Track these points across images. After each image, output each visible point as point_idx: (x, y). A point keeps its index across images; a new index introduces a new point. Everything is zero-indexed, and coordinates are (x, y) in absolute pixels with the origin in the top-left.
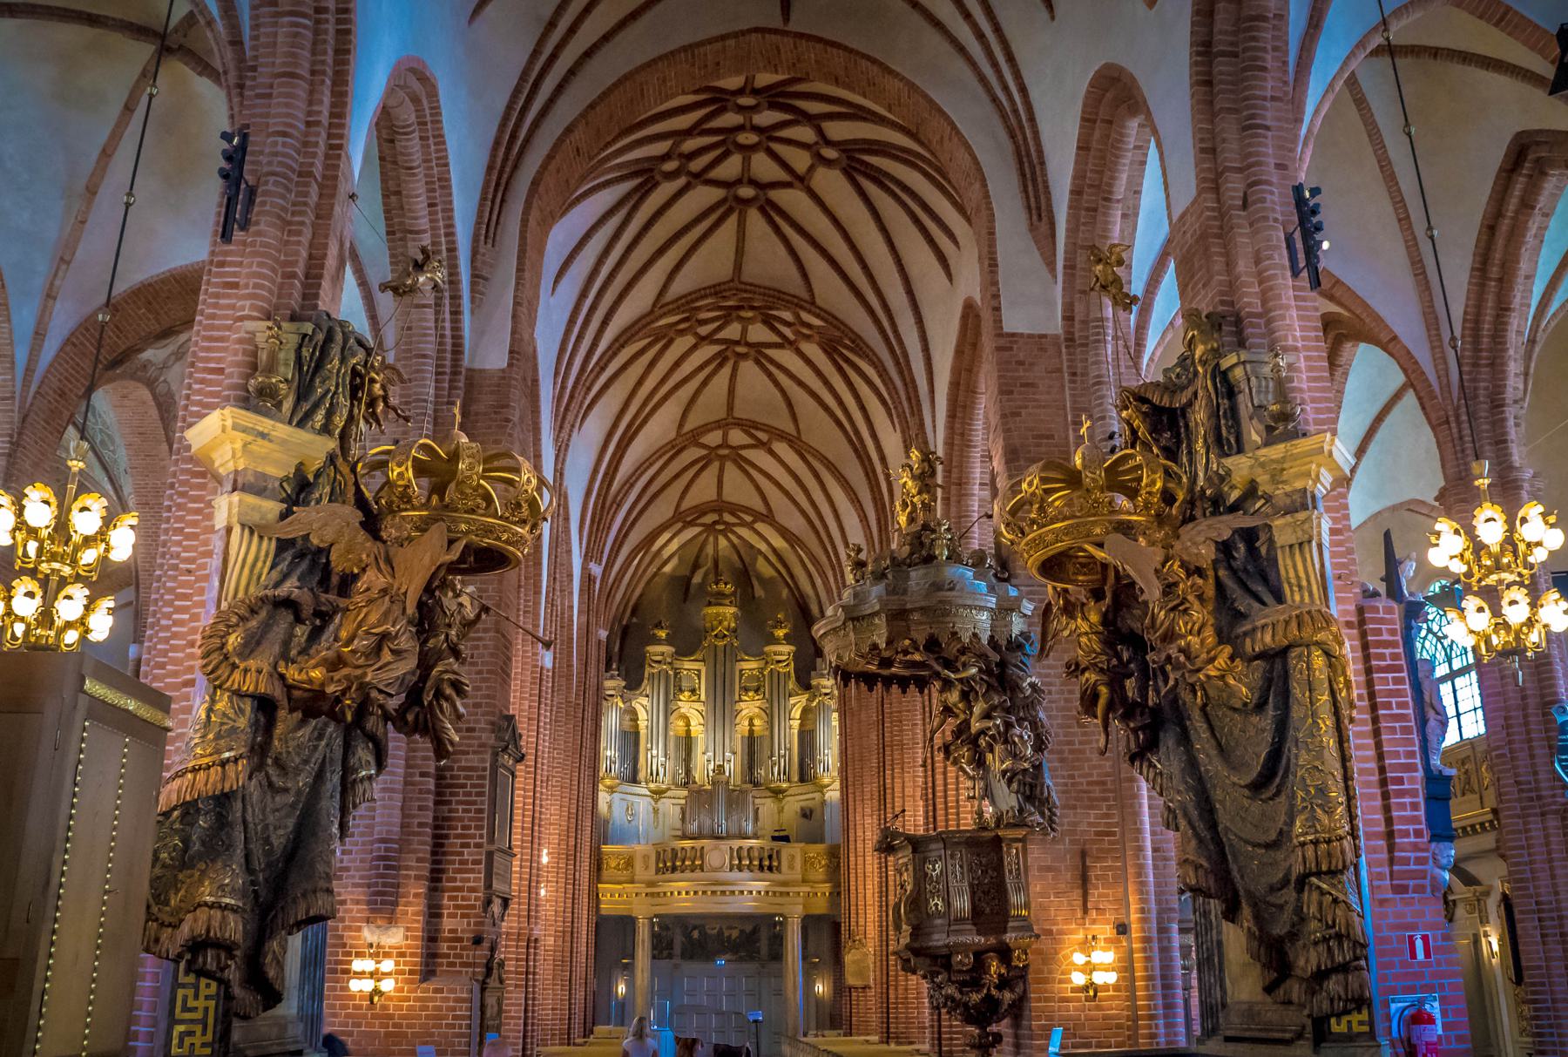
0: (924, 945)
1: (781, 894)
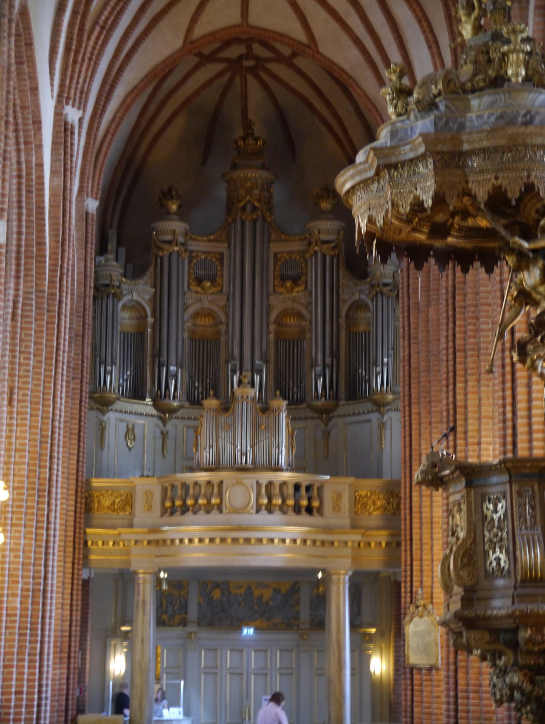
0: (480, 612)
1: (323, 543)
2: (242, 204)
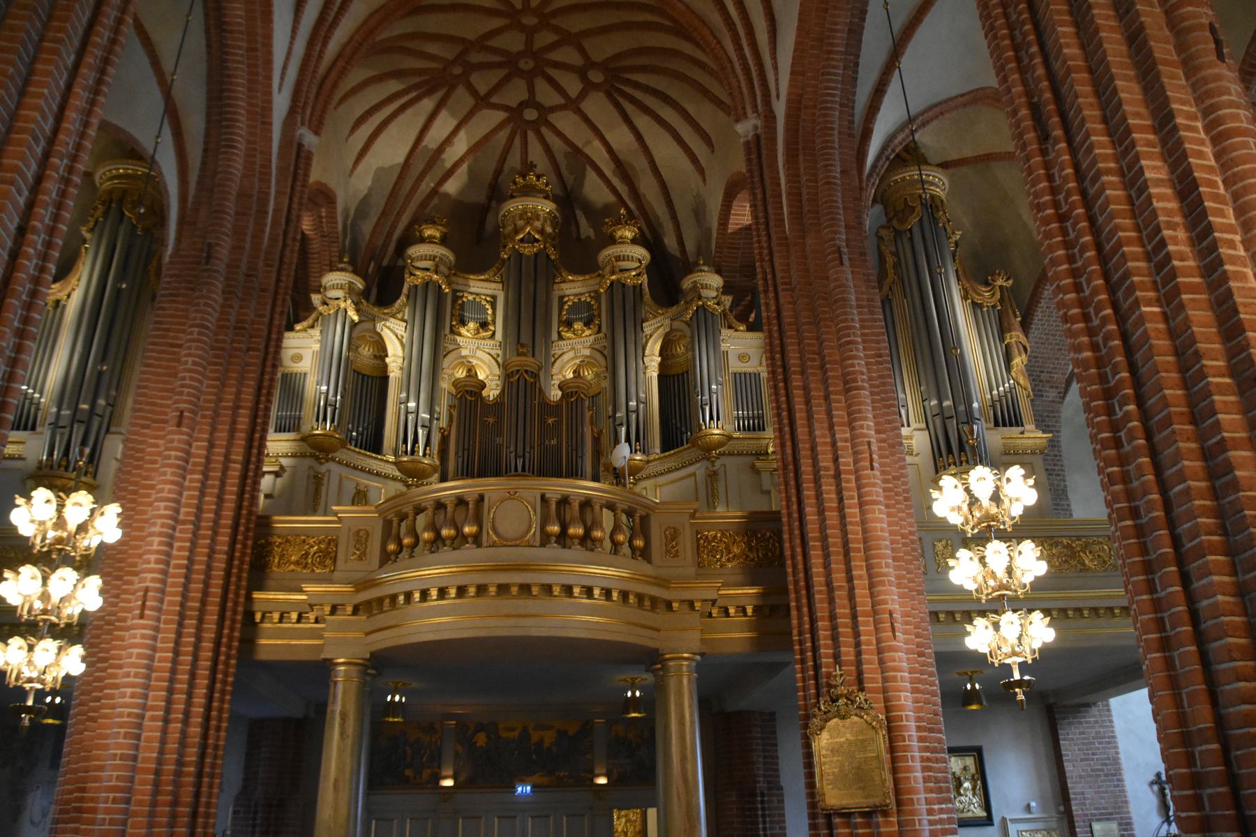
1: (654, 600)
2: (521, 236)
